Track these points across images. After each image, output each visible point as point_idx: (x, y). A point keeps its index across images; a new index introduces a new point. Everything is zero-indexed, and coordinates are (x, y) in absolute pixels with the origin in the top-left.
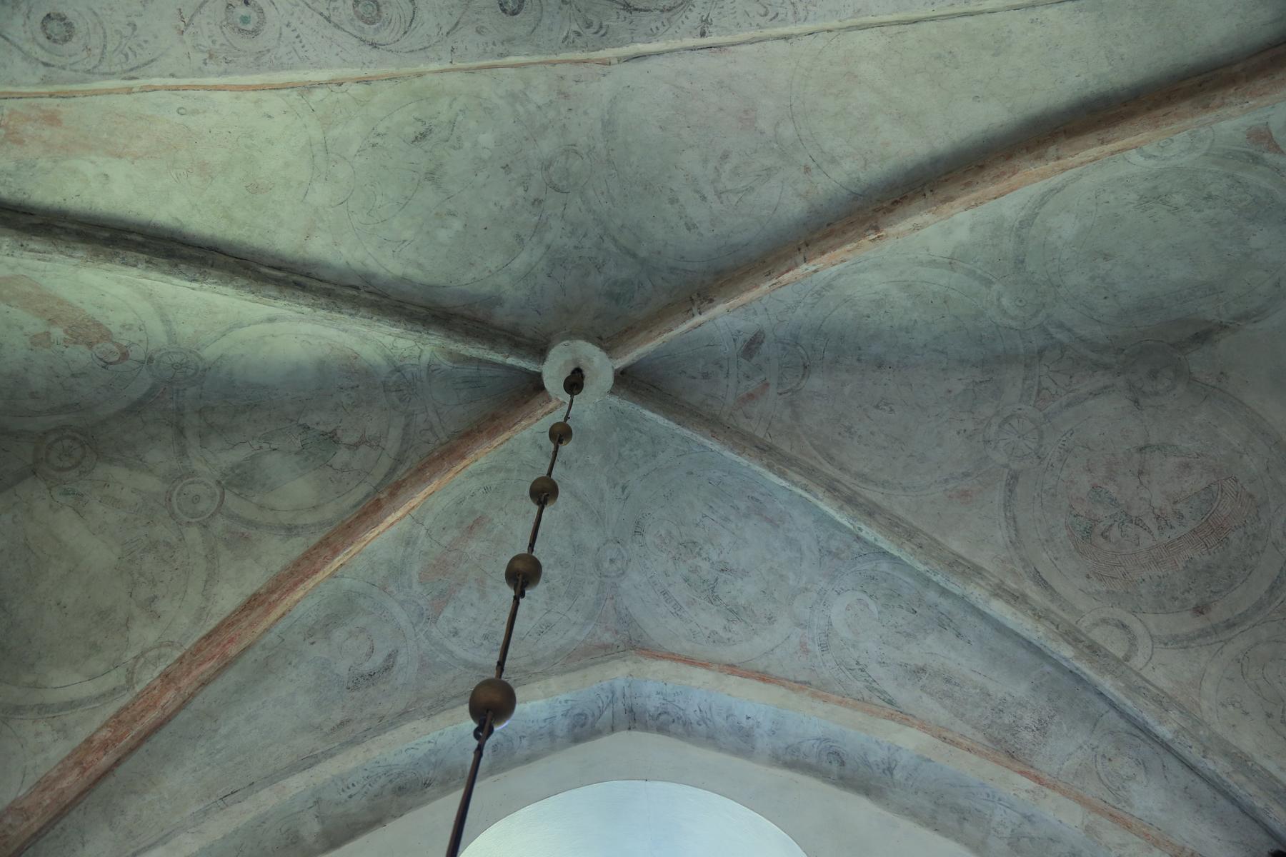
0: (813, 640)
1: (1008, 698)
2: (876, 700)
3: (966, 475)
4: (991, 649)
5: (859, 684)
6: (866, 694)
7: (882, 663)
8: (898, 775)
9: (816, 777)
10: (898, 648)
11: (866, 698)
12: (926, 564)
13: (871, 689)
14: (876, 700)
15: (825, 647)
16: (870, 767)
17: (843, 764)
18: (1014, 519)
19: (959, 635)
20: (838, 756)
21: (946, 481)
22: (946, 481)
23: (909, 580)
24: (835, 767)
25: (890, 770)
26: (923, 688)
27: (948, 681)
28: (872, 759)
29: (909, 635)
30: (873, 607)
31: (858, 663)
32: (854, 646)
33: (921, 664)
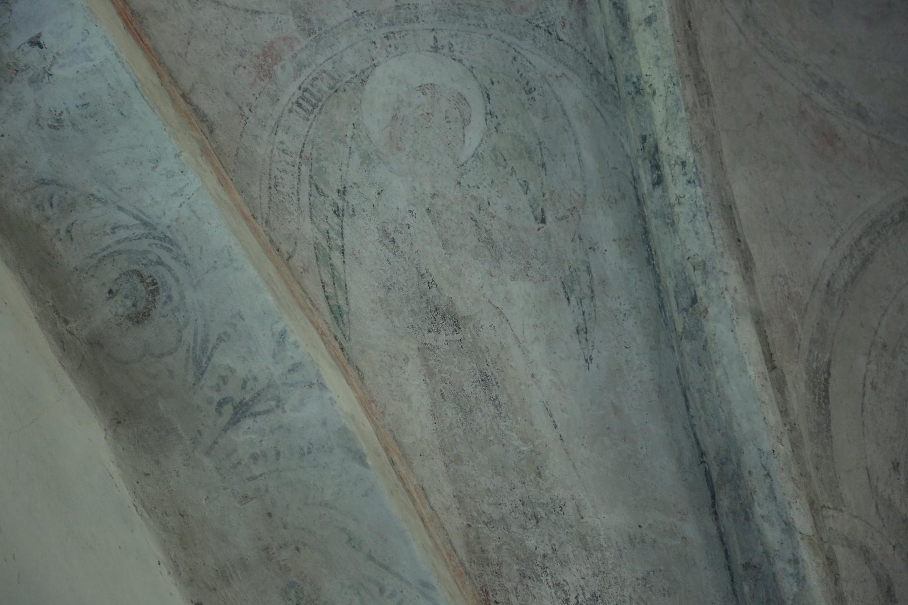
0: (300, 67)
1: (570, 509)
2: (311, 283)
3: (860, 113)
4: (617, 410)
5: (307, 228)
6: (303, 255)
7: (388, 239)
8: (246, 437)
9: (34, 294)
10: (445, 244)
11: (296, 261)
12: (695, 148)
13: (321, 256)
14: (311, 283)
15: (309, 103)
16: (200, 373)
17: (140, 317)
18: (867, 260)
19: (581, 331)
20: (147, 293)
21: (823, 85)
22: (823, 85)
23: (589, 160)
24: (107, 312)
25: (241, 411)
26: (425, 350)
27: (485, 381)
28: (223, 359)
29: (490, 243)
30: (474, 137)
31: (343, 192)
32: (366, 158)
33: (462, 308)
